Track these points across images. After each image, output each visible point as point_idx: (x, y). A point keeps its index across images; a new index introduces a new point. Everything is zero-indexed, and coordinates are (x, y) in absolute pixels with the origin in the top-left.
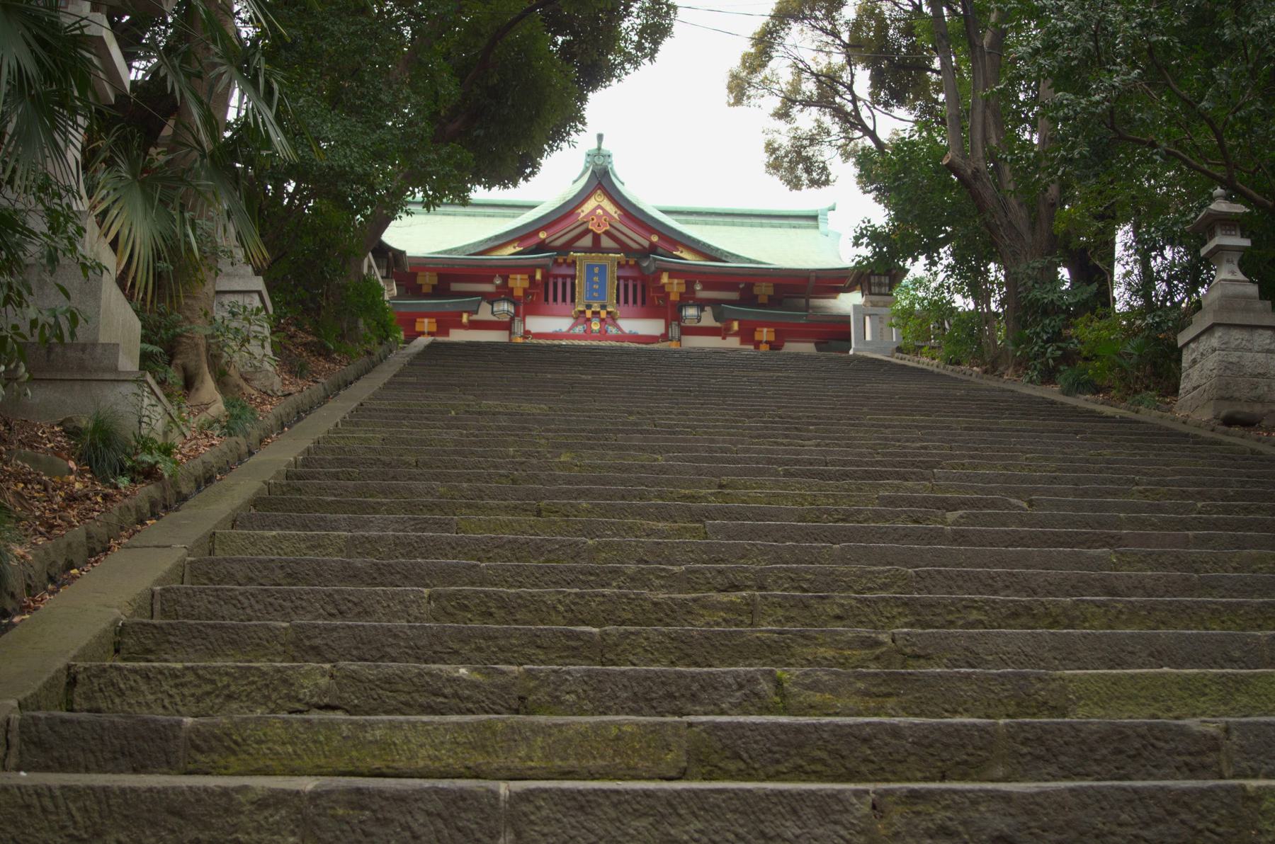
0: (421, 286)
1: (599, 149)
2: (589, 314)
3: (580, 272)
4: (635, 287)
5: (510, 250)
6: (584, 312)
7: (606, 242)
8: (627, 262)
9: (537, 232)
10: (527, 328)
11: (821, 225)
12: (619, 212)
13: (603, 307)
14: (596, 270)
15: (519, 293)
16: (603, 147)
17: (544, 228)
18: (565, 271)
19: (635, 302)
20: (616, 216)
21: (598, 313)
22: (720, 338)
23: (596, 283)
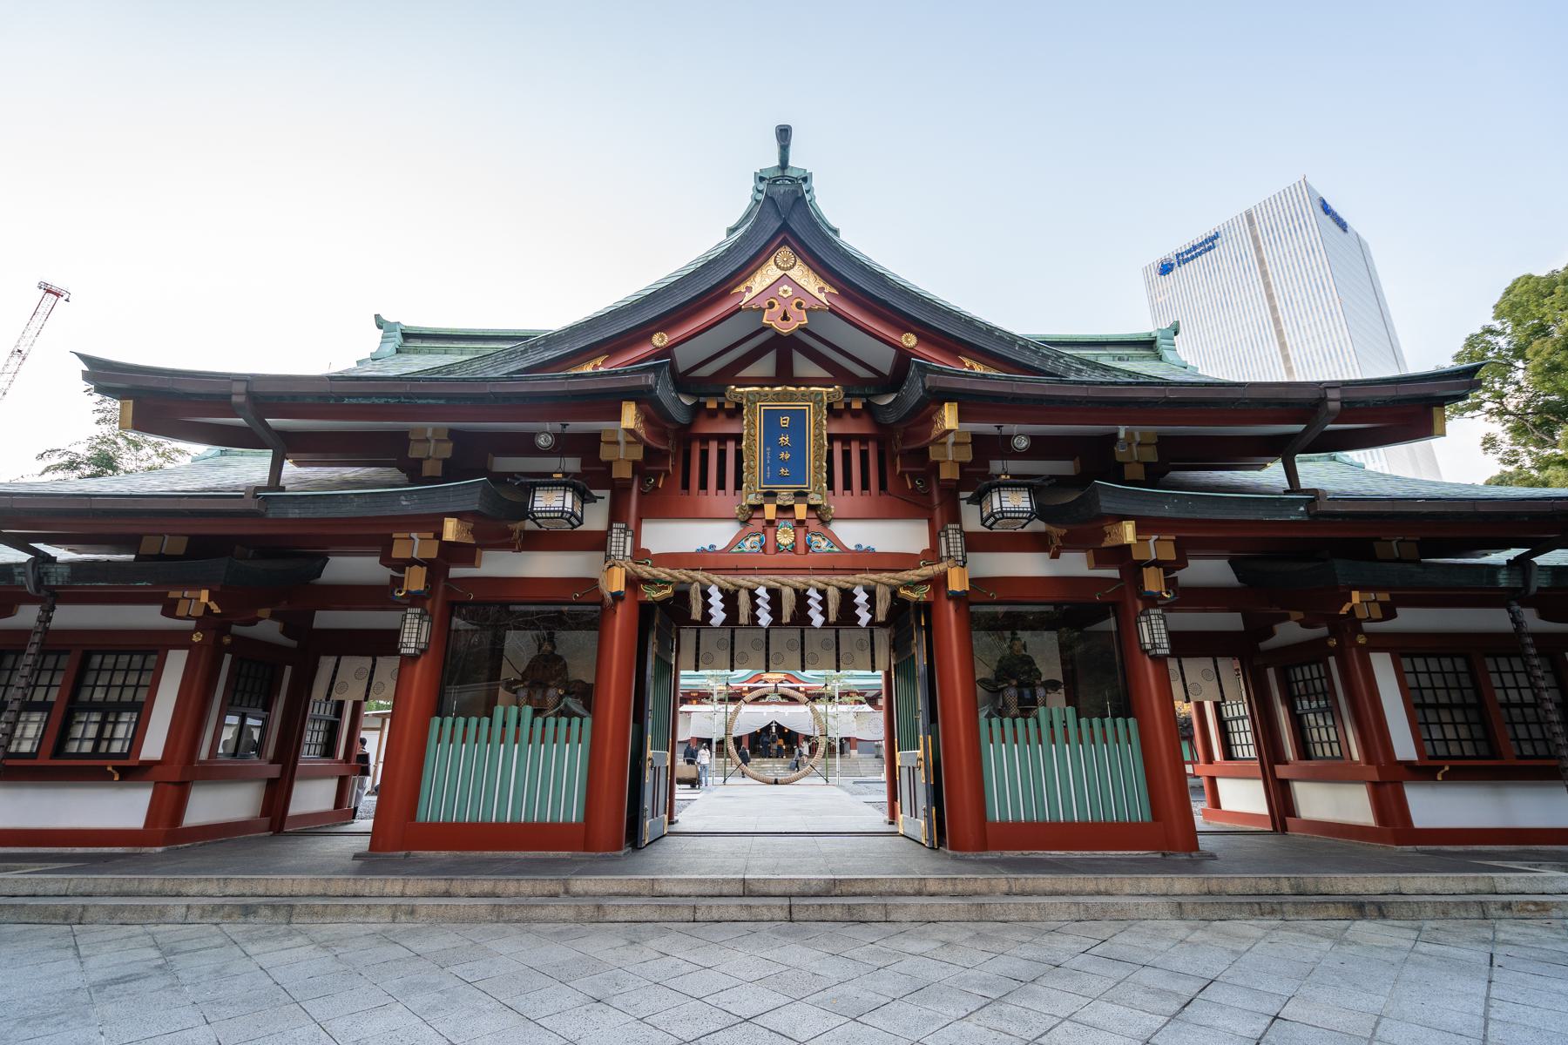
1: (784, 164)
2: (770, 511)
3: (752, 427)
4: (864, 456)
6: (760, 508)
7: (803, 367)
8: (848, 405)
9: (641, 334)
10: (644, 545)
11: (1167, 354)
12: (828, 289)
13: (801, 495)
14: (785, 422)
15: (623, 472)
16: (791, 163)
17: (667, 321)
19: (865, 485)
20: (822, 297)
21: (791, 508)
22: (1046, 555)
23: (784, 448)
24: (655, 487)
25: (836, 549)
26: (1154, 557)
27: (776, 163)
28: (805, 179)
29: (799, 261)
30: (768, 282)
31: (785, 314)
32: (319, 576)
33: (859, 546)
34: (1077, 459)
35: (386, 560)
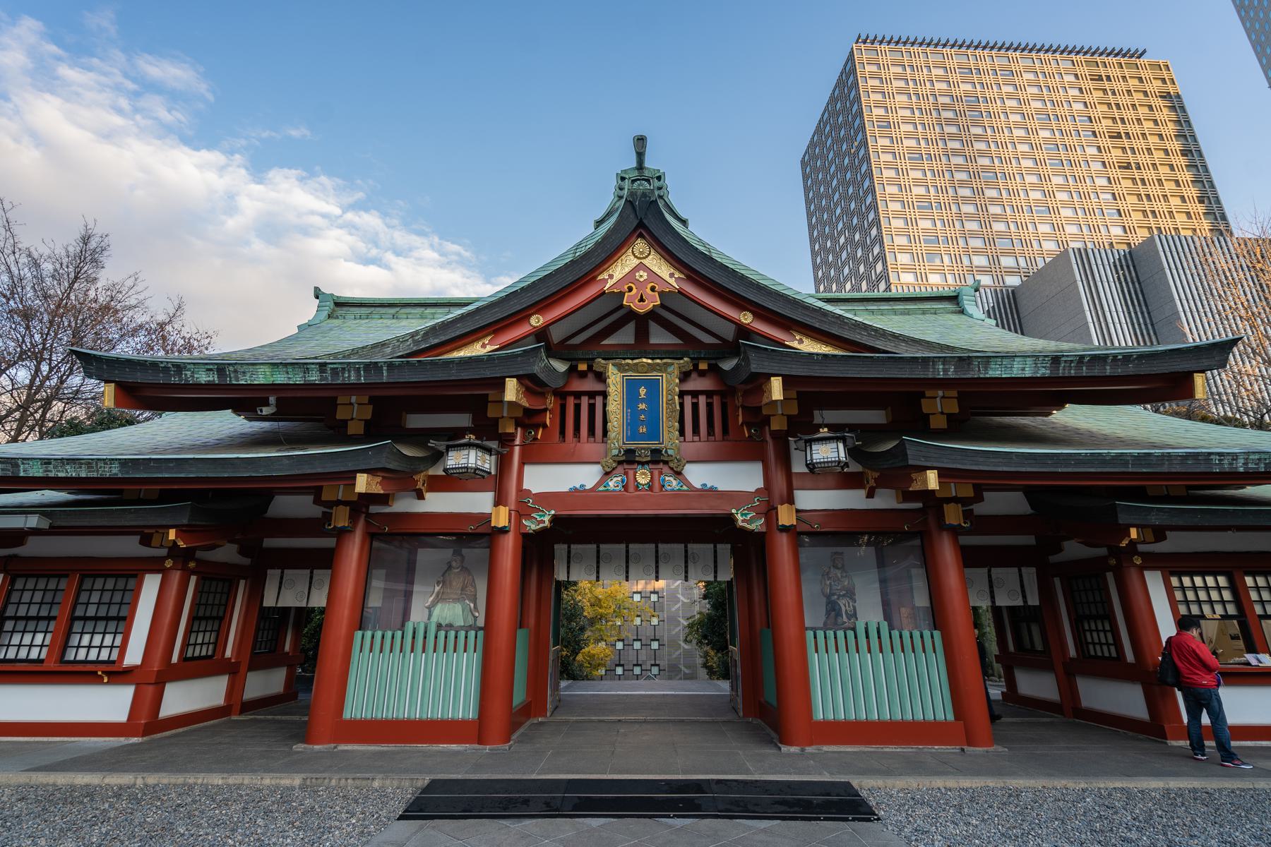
0: (345, 423)
1: (640, 167)
4: (710, 406)
5: (476, 350)
9: (521, 316)
10: (525, 486)
17: (542, 306)
18: (589, 385)
20: (672, 281)
22: (862, 493)
24: (535, 439)
25: (685, 488)
26: (954, 494)
27: (634, 165)
28: (659, 178)
29: (652, 251)
30: (627, 270)
31: (642, 296)
32: (266, 512)
33: (705, 485)
34: (889, 408)
35: (318, 501)
